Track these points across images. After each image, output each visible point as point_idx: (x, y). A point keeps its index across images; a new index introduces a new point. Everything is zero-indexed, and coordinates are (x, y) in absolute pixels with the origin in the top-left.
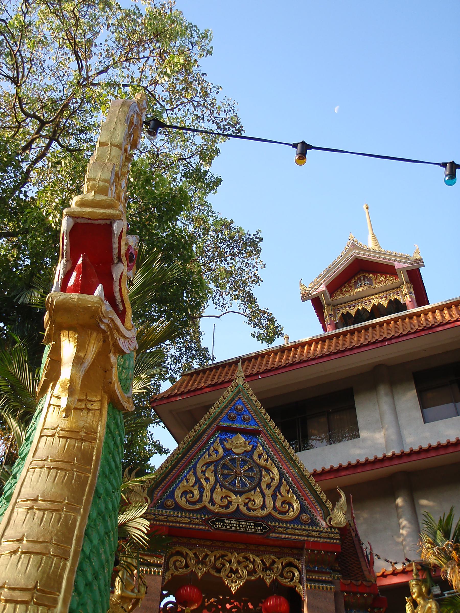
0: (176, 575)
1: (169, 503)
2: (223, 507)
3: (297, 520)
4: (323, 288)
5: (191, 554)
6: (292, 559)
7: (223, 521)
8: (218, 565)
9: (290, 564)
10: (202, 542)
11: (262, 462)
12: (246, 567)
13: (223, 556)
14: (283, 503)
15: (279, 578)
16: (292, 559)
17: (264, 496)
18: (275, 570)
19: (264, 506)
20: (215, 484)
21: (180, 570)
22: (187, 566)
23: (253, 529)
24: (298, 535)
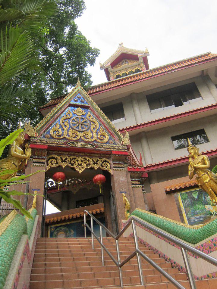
0: (52, 167)
1: (47, 136)
2: (73, 137)
3: (107, 142)
4: (109, 64)
5: (59, 158)
6: (106, 159)
7: (74, 143)
8: (72, 162)
9: (105, 161)
10: (63, 153)
11: (90, 119)
12: (85, 163)
13: (74, 159)
14: (101, 135)
15: (101, 167)
16: (106, 159)
17: (92, 132)
18: (99, 164)
19: (92, 137)
20: (69, 128)
21: (54, 165)
22: (57, 163)
23: (88, 146)
24: (108, 148)
